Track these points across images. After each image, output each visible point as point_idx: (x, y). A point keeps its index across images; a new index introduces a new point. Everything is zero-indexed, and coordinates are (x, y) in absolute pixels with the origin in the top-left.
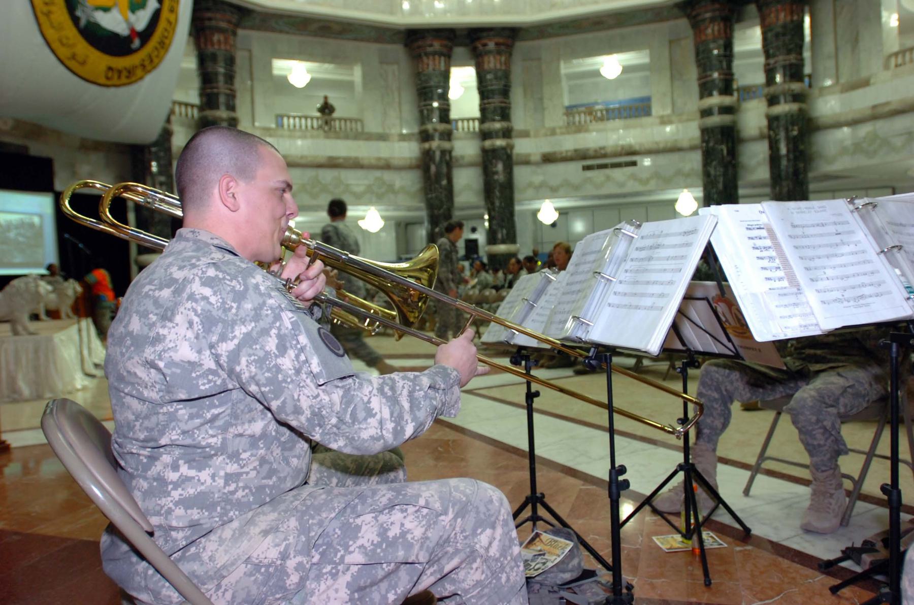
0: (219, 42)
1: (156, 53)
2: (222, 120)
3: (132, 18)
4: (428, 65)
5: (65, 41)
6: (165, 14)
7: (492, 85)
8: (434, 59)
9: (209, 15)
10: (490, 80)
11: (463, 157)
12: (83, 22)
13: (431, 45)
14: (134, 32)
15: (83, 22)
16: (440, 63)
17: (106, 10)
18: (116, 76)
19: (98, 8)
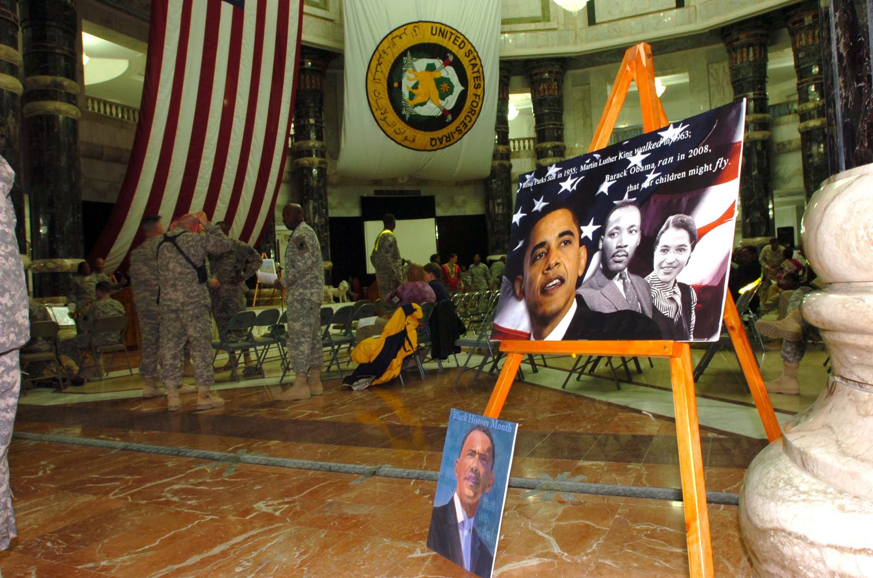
0: (544, 90)
1: (468, 119)
2: (548, 149)
3: (443, 103)
4: (736, 59)
5: (398, 131)
6: (471, 90)
7: (804, 64)
8: (742, 53)
9: (535, 72)
10: (803, 58)
11: (790, 142)
12: (408, 116)
13: (738, 39)
14: (445, 112)
15: (408, 116)
16: (748, 54)
17: (423, 104)
18: (438, 142)
19: (416, 106)
